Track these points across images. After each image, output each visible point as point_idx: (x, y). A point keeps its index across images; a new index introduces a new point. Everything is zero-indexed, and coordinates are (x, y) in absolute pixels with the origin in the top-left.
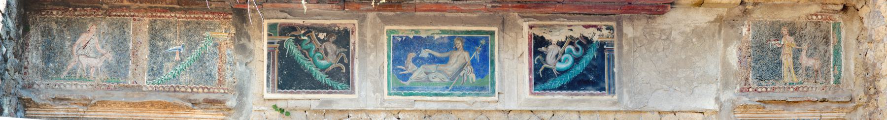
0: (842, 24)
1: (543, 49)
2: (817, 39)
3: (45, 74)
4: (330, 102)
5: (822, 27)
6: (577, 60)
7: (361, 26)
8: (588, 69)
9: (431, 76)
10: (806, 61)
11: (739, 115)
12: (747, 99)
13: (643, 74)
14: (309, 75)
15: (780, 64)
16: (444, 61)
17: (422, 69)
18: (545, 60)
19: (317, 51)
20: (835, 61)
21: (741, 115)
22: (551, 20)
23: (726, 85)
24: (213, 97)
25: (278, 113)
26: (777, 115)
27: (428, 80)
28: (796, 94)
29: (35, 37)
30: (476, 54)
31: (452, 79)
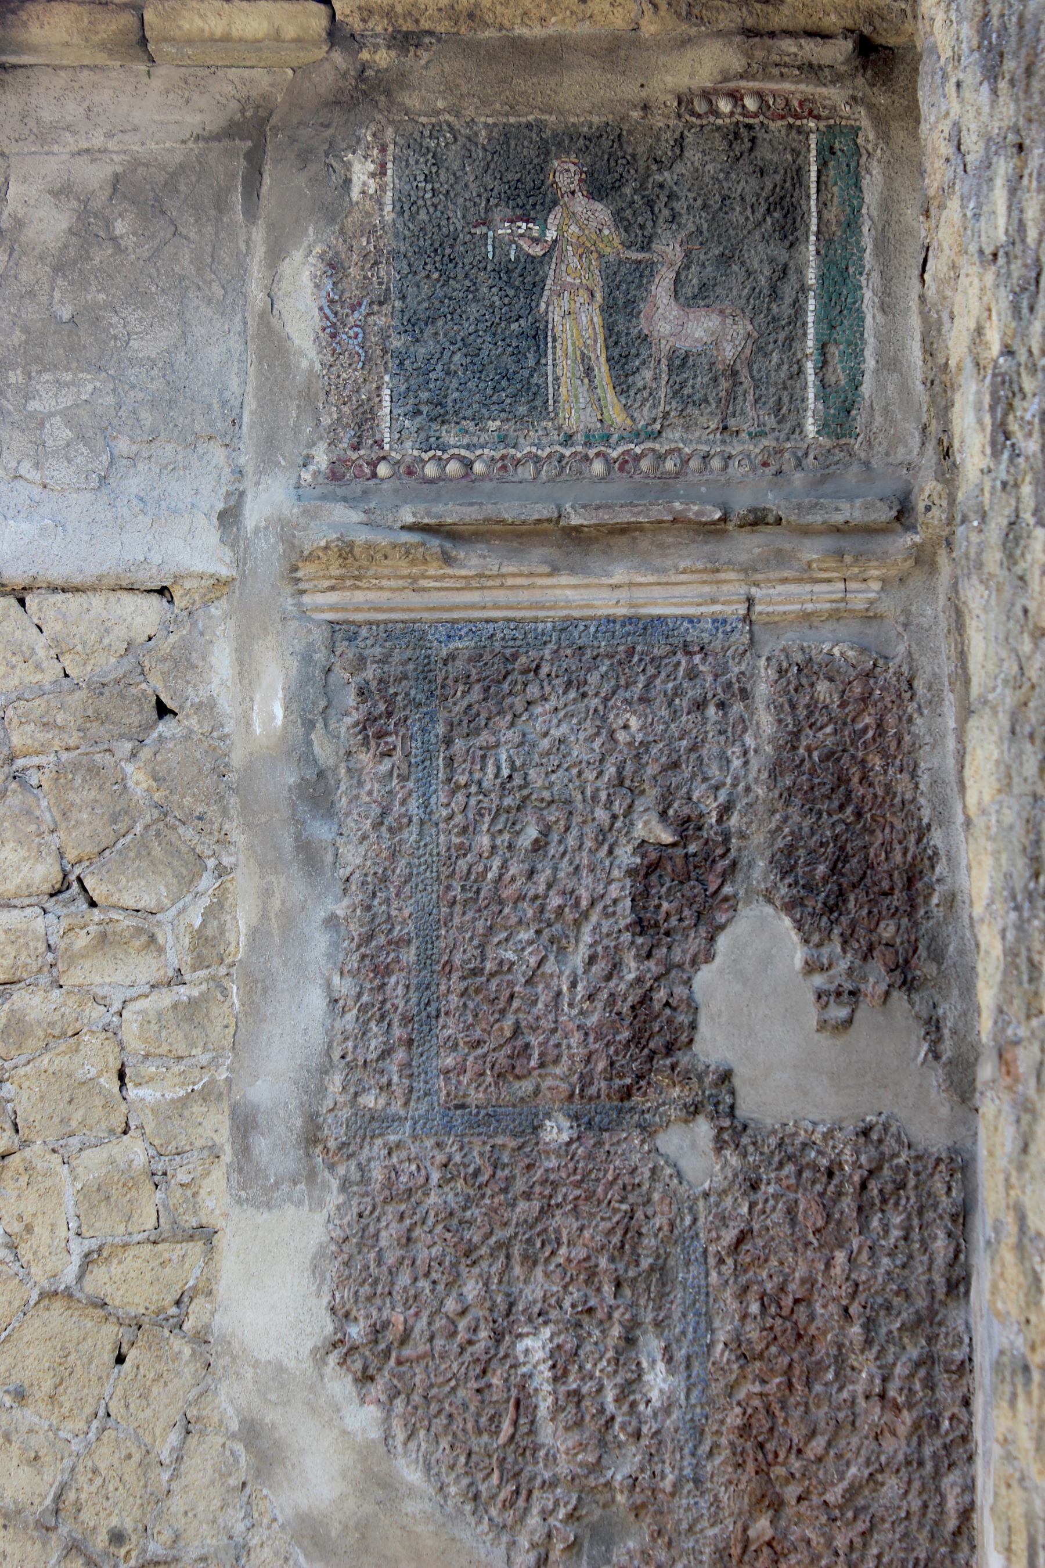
0: (868, 134)
2: (736, 216)
5: (765, 153)
11: (321, 599)
12: (355, 516)
21: (333, 598)
26: (524, 596)
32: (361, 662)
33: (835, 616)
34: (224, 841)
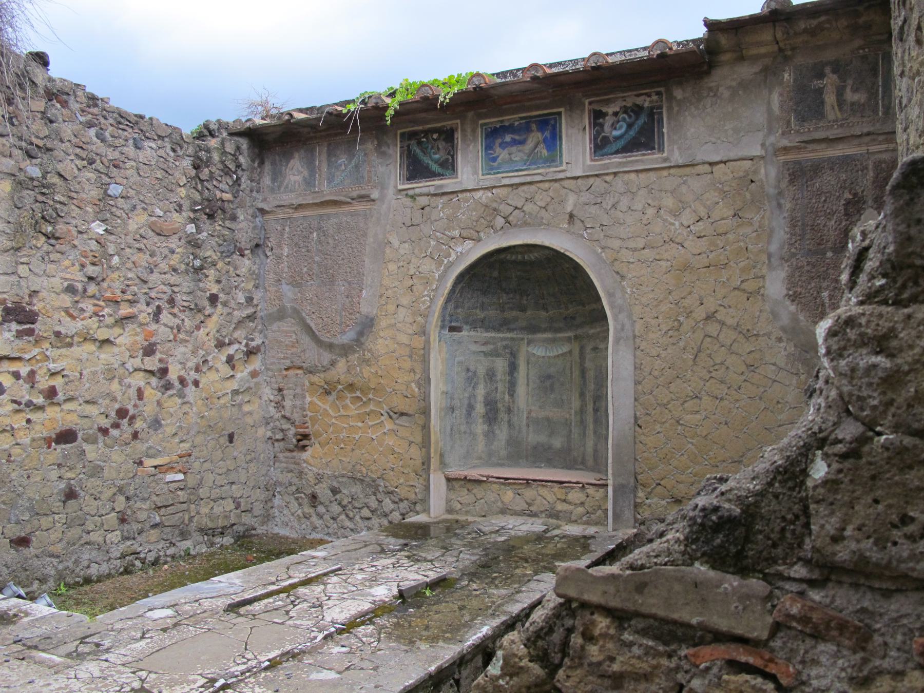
1: (601, 120)
3: (272, 190)
4: (441, 186)
6: (630, 126)
7: (462, 124)
8: (641, 132)
9: (513, 156)
10: (851, 96)
13: (692, 130)
14: (427, 168)
15: (822, 103)
16: (522, 142)
17: (506, 151)
18: (603, 131)
19: (432, 148)
20: (884, 92)
22: (606, 94)
23: (770, 131)
24: (363, 192)
25: (409, 199)
27: (511, 159)
28: (840, 130)
29: (267, 167)
30: (547, 134)
31: (529, 156)
32: (788, 170)
33: (886, 151)
34: (764, 204)
